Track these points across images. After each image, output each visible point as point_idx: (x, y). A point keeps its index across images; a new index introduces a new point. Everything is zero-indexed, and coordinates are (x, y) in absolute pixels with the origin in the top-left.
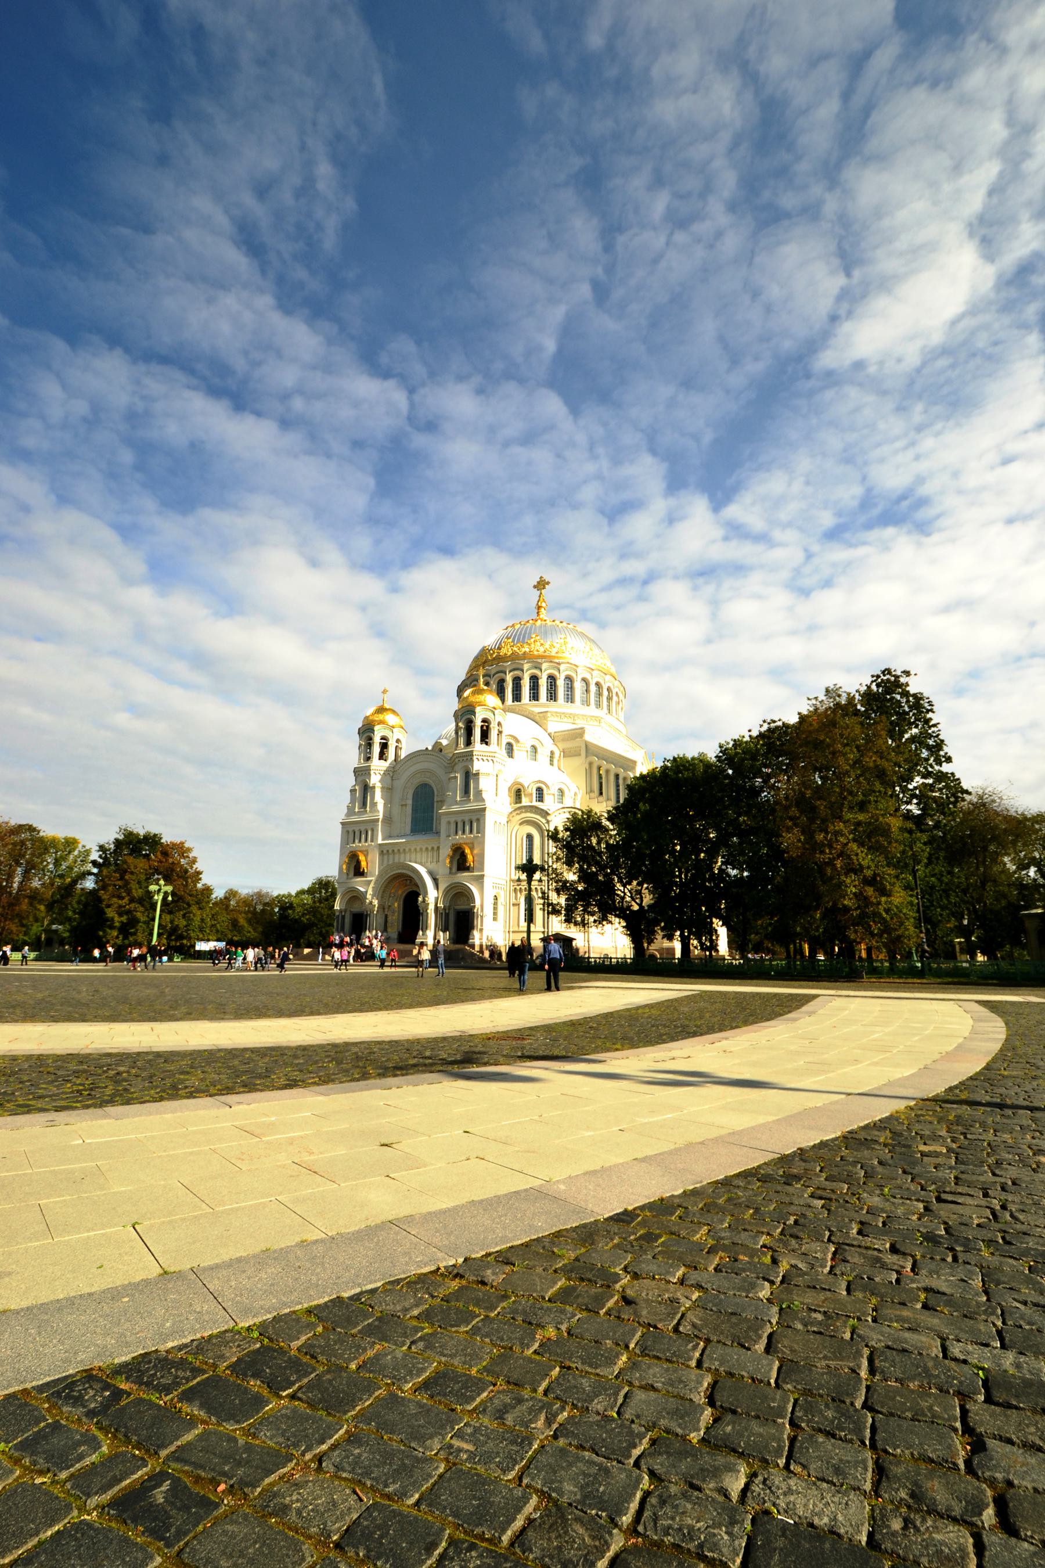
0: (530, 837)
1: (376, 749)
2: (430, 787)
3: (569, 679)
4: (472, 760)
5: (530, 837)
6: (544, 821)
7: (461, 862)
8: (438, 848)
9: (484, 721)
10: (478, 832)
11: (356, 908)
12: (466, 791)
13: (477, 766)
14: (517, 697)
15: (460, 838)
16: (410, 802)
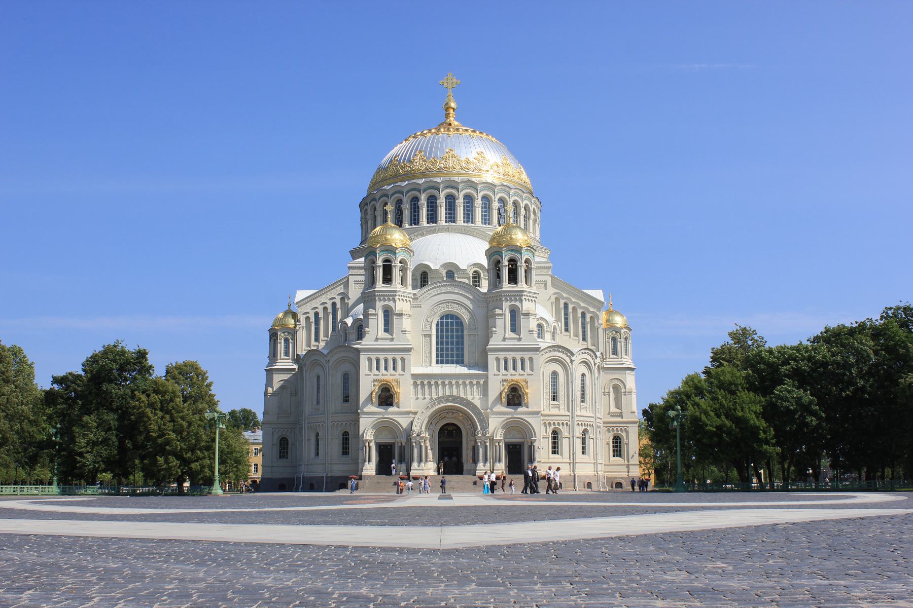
0: (555, 374)
1: (380, 273)
2: (457, 318)
3: (486, 199)
4: (521, 301)
5: (555, 374)
6: (568, 359)
7: (515, 397)
8: (486, 383)
9: (527, 261)
10: (532, 370)
11: (386, 439)
12: (515, 328)
13: (526, 306)
14: (469, 218)
15: (516, 376)
16: (434, 332)
